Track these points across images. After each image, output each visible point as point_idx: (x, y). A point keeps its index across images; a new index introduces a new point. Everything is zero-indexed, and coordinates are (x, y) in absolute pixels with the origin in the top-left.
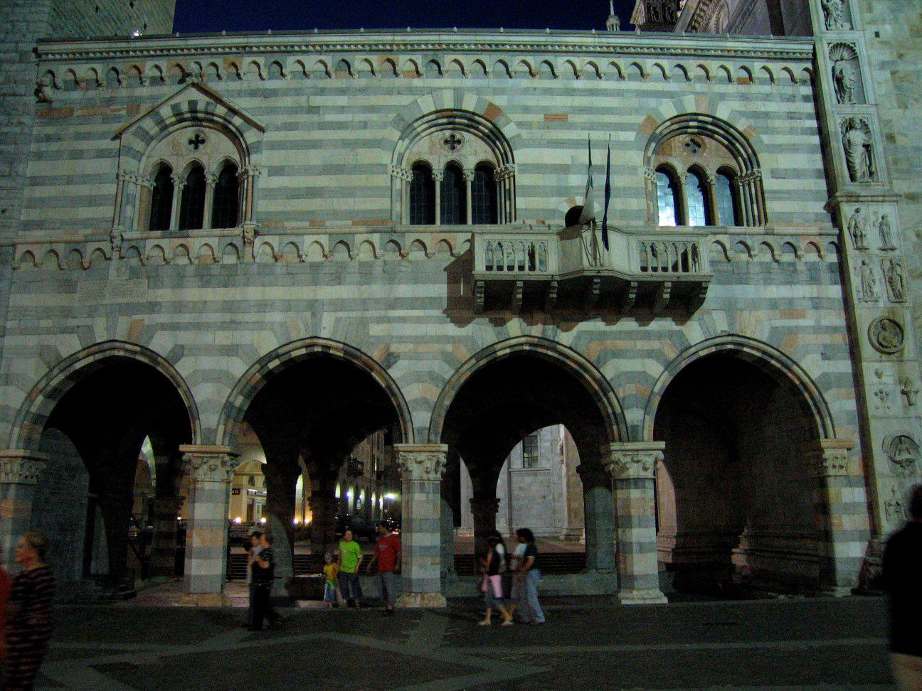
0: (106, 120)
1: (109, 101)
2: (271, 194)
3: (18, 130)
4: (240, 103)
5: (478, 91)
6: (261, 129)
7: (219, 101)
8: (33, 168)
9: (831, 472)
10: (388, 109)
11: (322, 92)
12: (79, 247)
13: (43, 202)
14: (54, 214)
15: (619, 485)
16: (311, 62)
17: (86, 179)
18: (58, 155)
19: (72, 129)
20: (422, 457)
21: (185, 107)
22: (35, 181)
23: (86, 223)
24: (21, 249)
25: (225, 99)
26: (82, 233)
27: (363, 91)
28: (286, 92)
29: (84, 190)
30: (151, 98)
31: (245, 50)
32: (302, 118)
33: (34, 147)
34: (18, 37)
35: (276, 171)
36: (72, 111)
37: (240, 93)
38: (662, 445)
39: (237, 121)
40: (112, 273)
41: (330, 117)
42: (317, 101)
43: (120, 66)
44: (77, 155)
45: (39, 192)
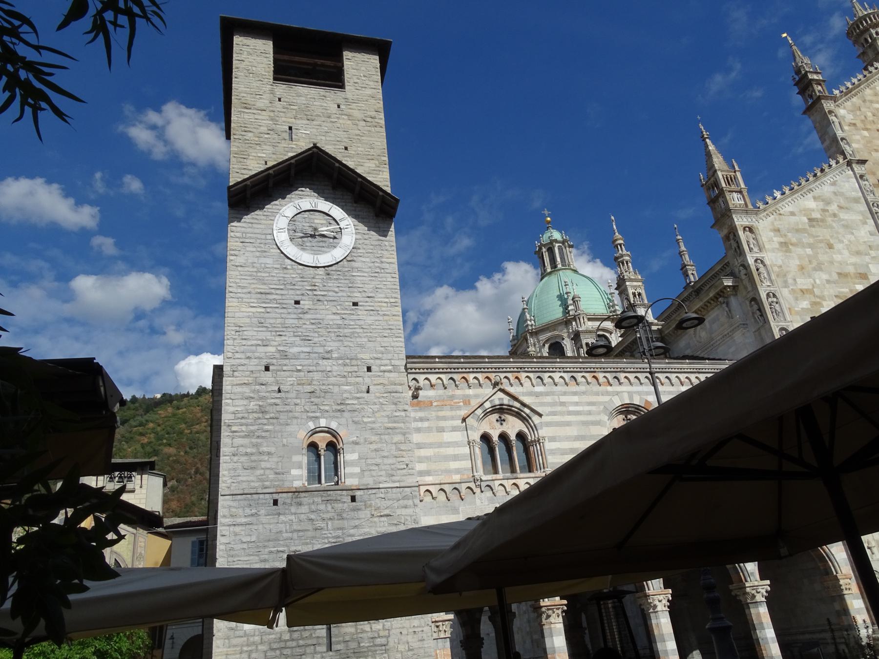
0: (452, 409)
1: (452, 397)
2: (553, 452)
3: (403, 414)
4: (526, 400)
5: (639, 393)
6: (540, 415)
7: (515, 399)
8: (416, 438)
9: (845, 592)
10: (600, 403)
11: (565, 394)
12: (457, 486)
13: (428, 459)
14: (433, 466)
15: (750, 605)
16: (556, 376)
17: (449, 444)
18: (429, 430)
19: (434, 414)
20: (661, 598)
21: (497, 402)
22: (420, 446)
23: (458, 471)
24: (423, 489)
25: (521, 398)
26: (456, 478)
27: (584, 393)
28: (547, 394)
29: (450, 451)
30: (476, 396)
31: (521, 369)
32: (559, 408)
33: (414, 425)
34: (390, 356)
35: (553, 439)
36: (431, 403)
37: (524, 394)
38: (768, 582)
39: (527, 411)
40: (478, 502)
41: (571, 408)
42: (563, 399)
43: (455, 376)
44: (441, 430)
45: (423, 452)
